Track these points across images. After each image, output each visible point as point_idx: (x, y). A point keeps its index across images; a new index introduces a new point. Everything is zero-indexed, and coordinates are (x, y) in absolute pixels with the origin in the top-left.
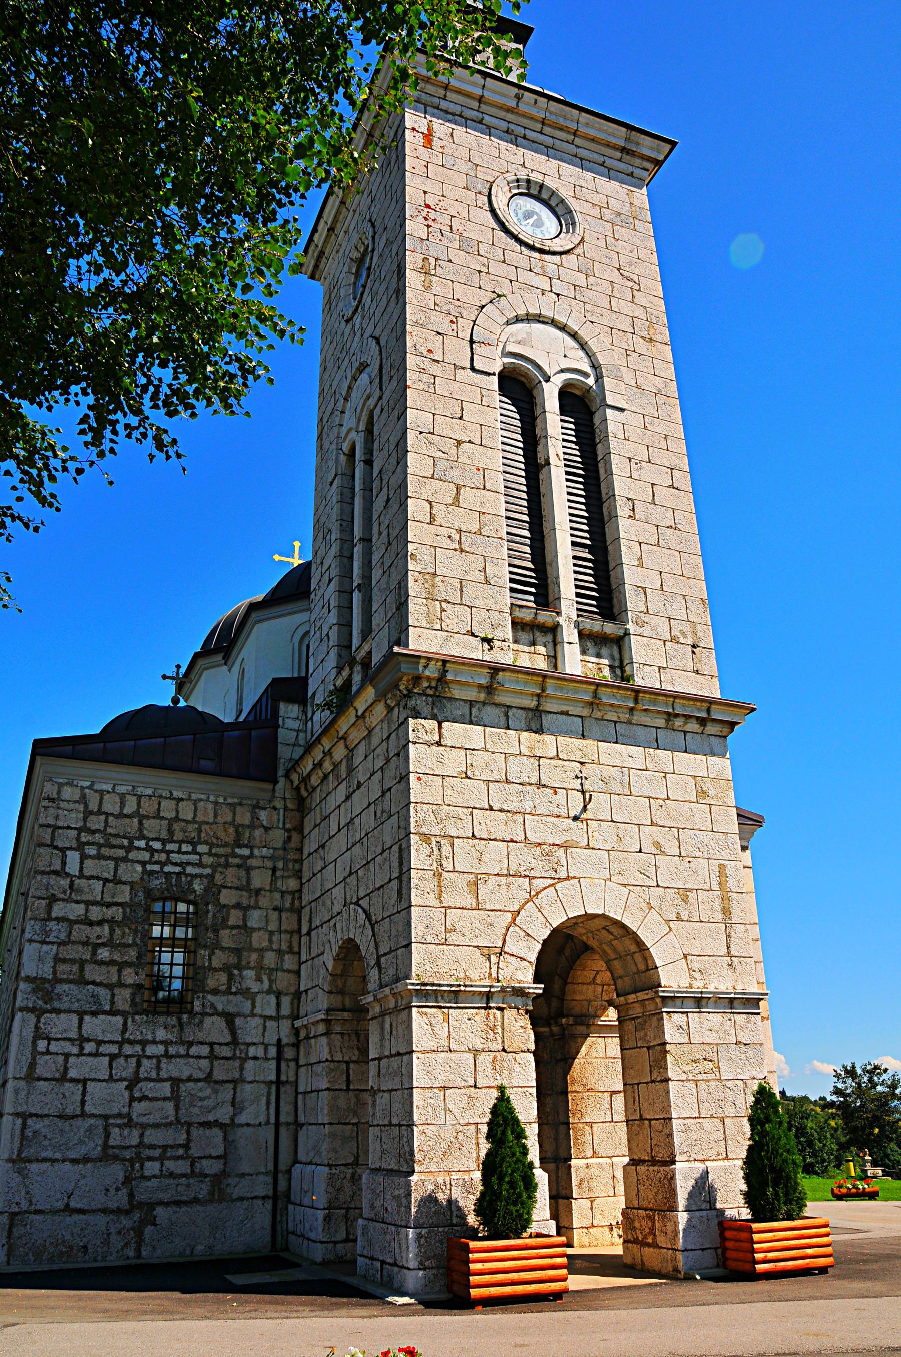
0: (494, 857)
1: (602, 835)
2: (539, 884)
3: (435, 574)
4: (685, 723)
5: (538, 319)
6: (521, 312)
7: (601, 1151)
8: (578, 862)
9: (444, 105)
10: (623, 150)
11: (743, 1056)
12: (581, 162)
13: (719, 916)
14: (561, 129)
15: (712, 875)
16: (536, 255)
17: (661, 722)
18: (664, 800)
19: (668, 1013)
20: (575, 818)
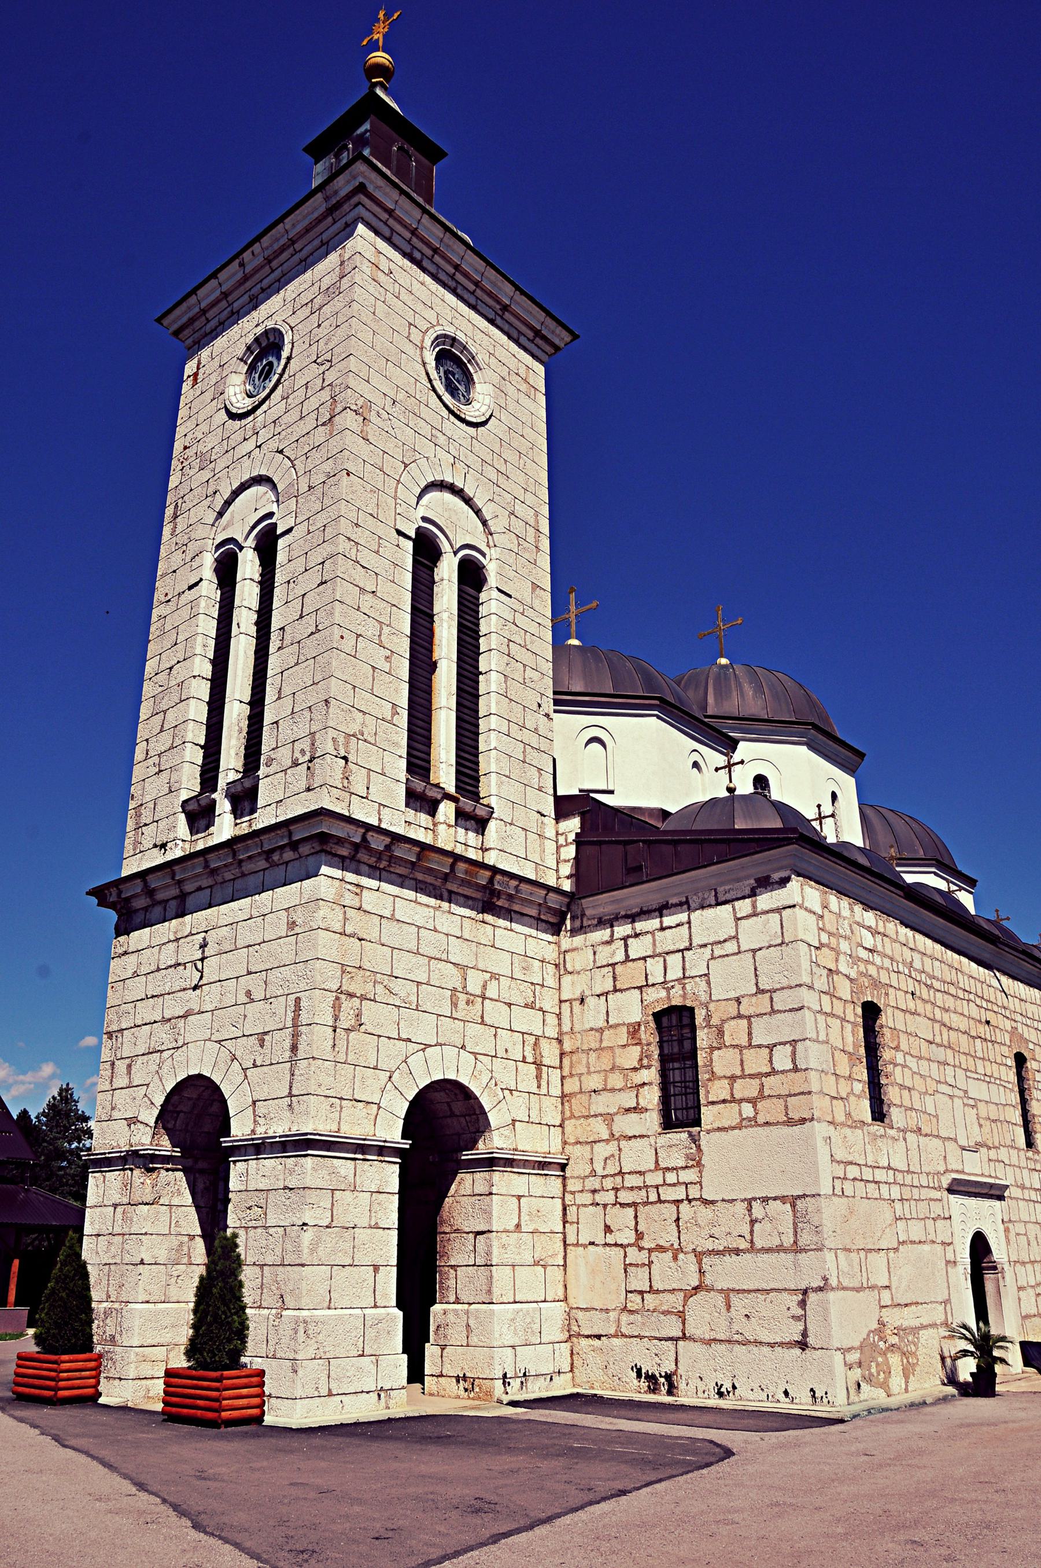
0: (143, 1039)
1: (210, 997)
2: (166, 1054)
3: (142, 805)
4: (281, 855)
5: (243, 487)
6: (226, 495)
7: (463, 1298)
8: (196, 1028)
9: (208, 328)
10: (330, 211)
11: (287, 1202)
12: (306, 264)
13: (288, 1054)
14: (282, 249)
15: (289, 1012)
16: (251, 418)
17: (262, 864)
18: (259, 944)
19: (235, 1162)
20: (196, 988)
